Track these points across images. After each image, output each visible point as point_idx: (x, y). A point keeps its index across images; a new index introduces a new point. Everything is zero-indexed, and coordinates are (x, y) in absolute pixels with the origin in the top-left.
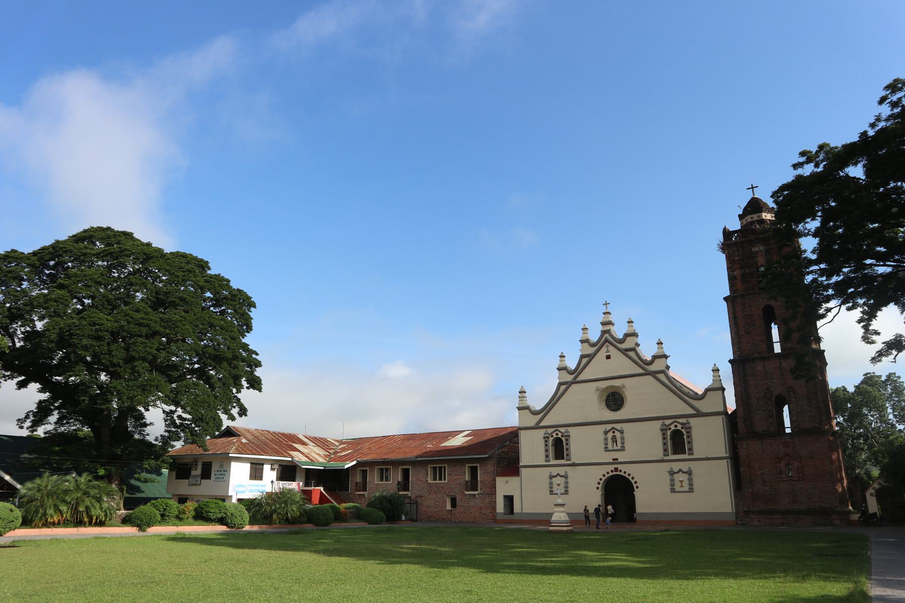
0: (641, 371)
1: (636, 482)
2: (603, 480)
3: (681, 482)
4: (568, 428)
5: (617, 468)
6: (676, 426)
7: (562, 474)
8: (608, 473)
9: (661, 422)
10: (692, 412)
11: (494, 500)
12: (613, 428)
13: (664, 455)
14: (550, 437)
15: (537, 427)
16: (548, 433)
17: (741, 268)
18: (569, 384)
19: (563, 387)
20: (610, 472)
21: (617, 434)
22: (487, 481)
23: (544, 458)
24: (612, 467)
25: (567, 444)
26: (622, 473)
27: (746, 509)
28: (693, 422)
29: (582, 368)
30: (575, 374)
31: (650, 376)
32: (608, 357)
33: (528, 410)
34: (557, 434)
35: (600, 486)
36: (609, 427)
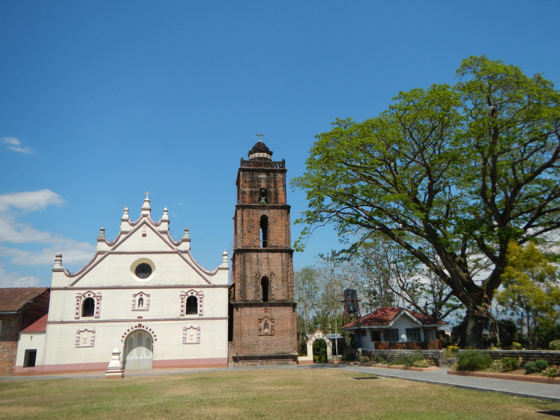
0: (171, 250)
1: (155, 336)
2: (127, 335)
3: (191, 336)
5: (141, 325)
6: (192, 293)
7: (89, 329)
8: (132, 328)
9: (181, 290)
10: (205, 283)
11: (14, 354)
12: (141, 292)
13: (181, 315)
14: (82, 297)
15: (71, 288)
16: (80, 294)
17: (250, 187)
18: (105, 254)
19: (100, 257)
21: (144, 297)
22: (8, 336)
23: (75, 315)
24: (137, 324)
25: (98, 303)
26: (145, 329)
27: (234, 355)
28: (205, 291)
30: (113, 247)
31: (177, 255)
32: (144, 235)
33: (63, 273)
34: (89, 295)
35: (124, 339)
36: (137, 291)
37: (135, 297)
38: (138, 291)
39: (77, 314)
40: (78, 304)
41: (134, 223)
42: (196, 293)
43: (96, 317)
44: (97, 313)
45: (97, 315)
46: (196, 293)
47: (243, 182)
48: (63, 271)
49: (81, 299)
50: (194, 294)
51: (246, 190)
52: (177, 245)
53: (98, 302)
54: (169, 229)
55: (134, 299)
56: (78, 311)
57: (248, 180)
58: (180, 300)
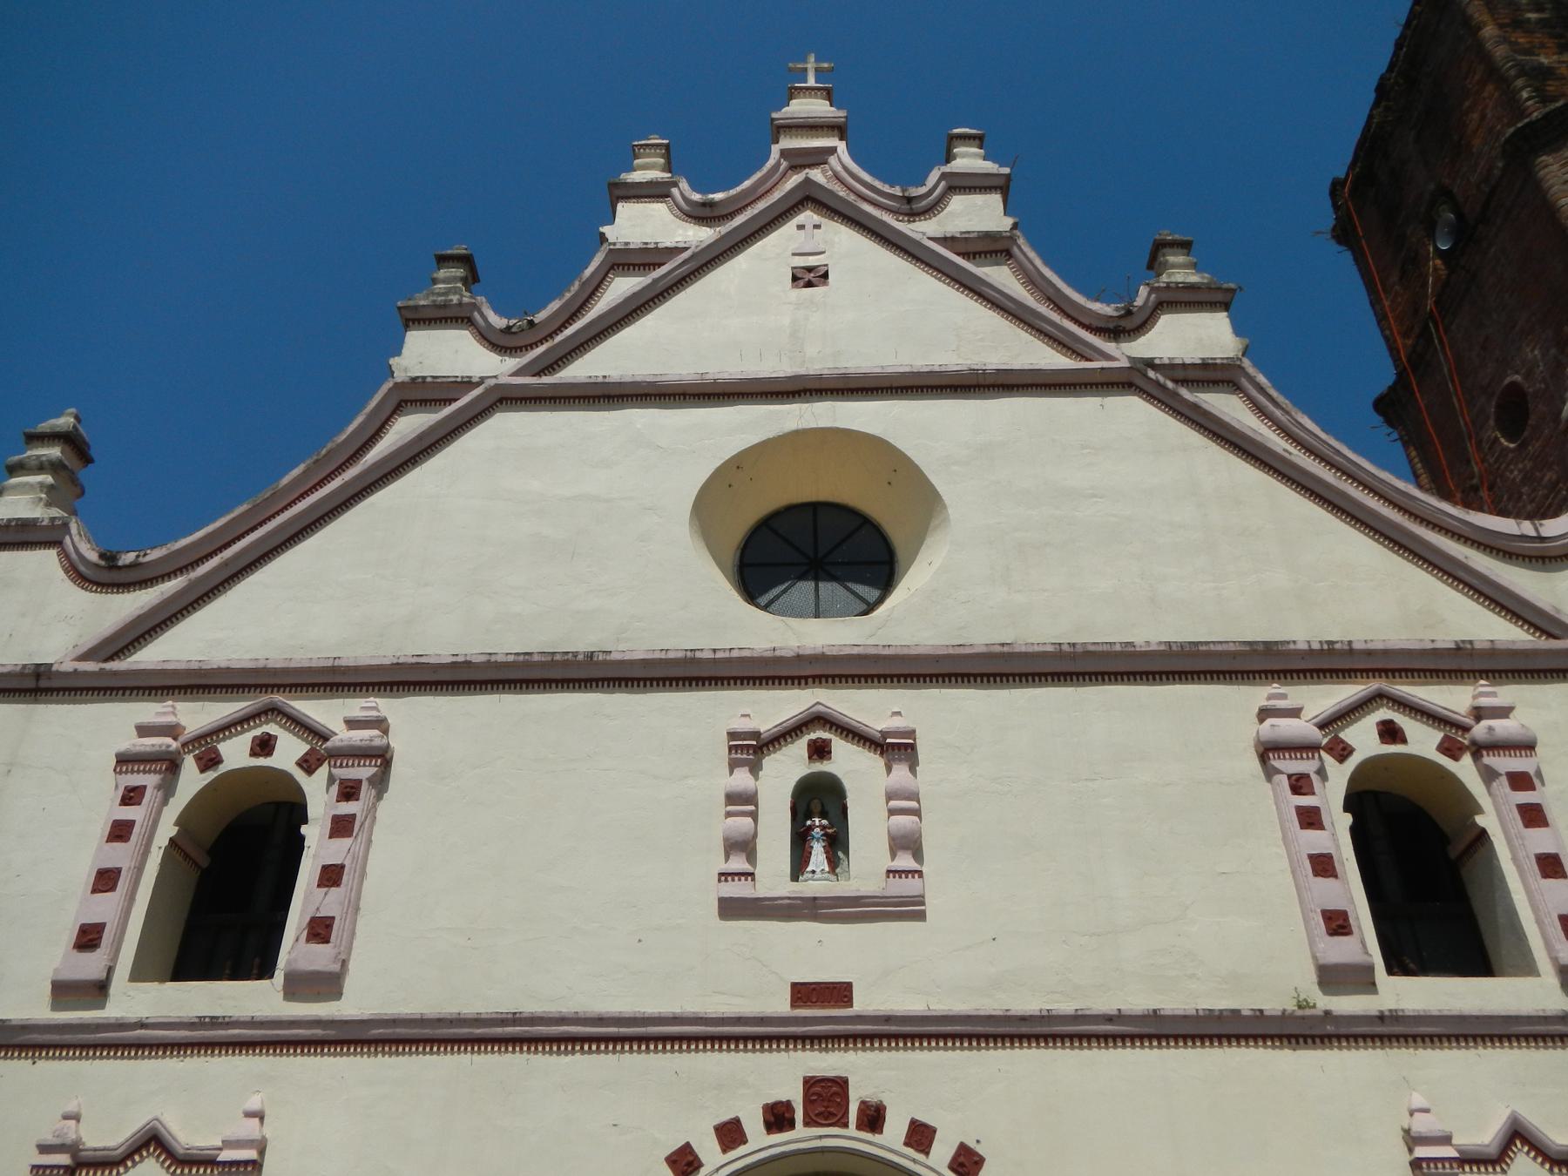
4: (384, 706)
5: (841, 1084)
6: (1390, 732)
8: (730, 1134)
9: (1259, 694)
12: (819, 719)
14: (189, 764)
16: (172, 730)
20: (754, 1125)
25: (341, 827)
29: (601, 317)
31: (1132, 409)
32: (810, 277)
33: (51, 555)
34: (264, 746)
37: (755, 769)
38: (786, 705)
39: (88, 938)
40: (120, 831)
41: (718, 196)
42: (1437, 736)
43: (302, 985)
44: (320, 930)
45: (319, 957)
46: (1437, 736)
47: (1501, 26)
48: (56, 543)
49: (168, 789)
50: (1423, 741)
51: (1544, 60)
52: (1117, 331)
53: (346, 808)
54: (1015, 226)
55: (742, 780)
56: (104, 908)
57: (1533, 16)
58: (1281, 802)
